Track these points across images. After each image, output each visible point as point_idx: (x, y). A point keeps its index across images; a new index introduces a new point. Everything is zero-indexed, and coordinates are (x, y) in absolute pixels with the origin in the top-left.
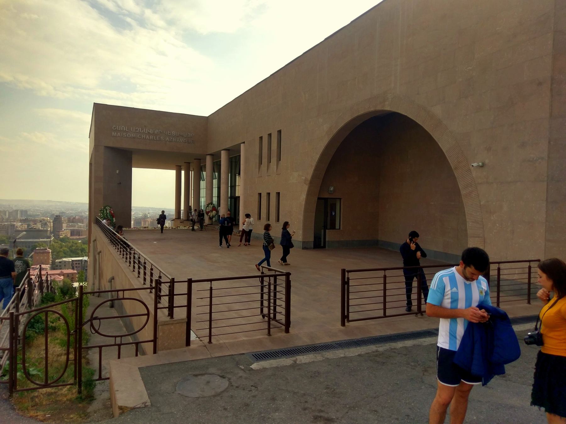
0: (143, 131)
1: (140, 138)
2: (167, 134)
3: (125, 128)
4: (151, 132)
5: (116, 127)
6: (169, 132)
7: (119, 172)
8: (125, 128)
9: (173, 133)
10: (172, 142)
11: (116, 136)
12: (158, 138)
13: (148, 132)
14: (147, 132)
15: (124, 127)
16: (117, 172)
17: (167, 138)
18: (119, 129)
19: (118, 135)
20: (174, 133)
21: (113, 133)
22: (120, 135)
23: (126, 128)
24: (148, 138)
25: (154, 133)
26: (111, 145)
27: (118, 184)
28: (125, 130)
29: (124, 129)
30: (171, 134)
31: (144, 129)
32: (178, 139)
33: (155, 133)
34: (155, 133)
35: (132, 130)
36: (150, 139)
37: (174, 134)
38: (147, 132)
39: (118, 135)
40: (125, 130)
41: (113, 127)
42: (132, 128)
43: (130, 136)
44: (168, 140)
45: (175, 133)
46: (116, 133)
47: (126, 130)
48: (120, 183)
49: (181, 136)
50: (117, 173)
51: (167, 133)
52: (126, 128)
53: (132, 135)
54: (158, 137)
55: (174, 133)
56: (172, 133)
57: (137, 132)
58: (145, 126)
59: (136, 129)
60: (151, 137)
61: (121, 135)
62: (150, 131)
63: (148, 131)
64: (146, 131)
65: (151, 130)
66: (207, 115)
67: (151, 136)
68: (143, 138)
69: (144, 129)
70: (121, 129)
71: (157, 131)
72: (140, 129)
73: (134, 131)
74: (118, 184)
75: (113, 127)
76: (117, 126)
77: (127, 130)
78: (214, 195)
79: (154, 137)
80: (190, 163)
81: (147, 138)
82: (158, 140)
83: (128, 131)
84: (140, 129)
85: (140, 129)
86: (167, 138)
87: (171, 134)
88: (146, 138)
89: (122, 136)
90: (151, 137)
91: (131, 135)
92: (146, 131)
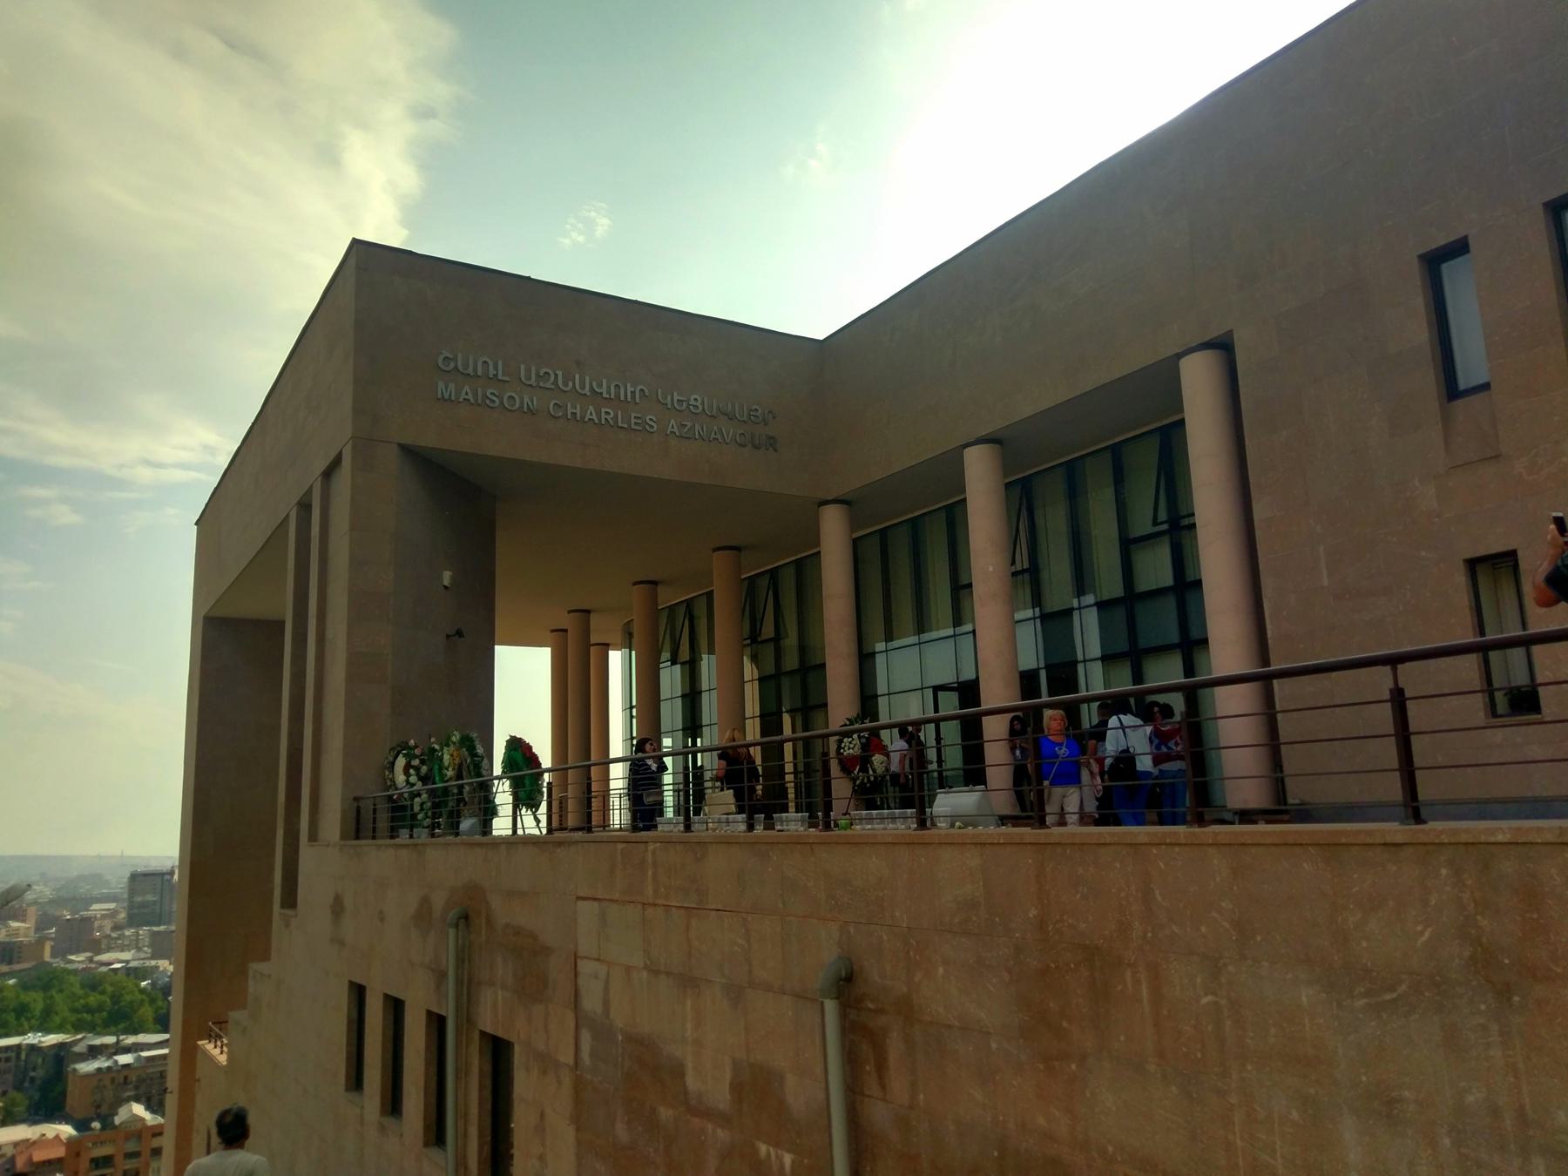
0: (570, 384)
1: (560, 414)
2: (669, 406)
3: (496, 368)
4: (604, 390)
5: (455, 359)
6: (676, 398)
7: (453, 578)
8: (496, 368)
9: (692, 402)
10: (689, 438)
11: (453, 398)
12: (633, 421)
13: (592, 388)
14: (587, 391)
15: (488, 360)
16: (447, 578)
17: (673, 421)
18: (466, 366)
19: (463, 396)
20: (696, 399)
21: (441, 385)
22: (470, 397)
23: (500, 363)
24: (594, 417)
25: (617, 395)
26: (428, 439)
27: (448, 636)
28: (496, 375)
29: (492, 372)
30: (685, 404)
31: (577, 376)
32: (715, 428)
33: (622, 398)
34: (622, 398)
35: (523, 379)
36: (603, 422)
37: (696, 407)
38: (587, 391)
39: (463, 396)
40: (496, 375)
41: (441, 358)
42: (522, 367)
43: (517, 405)
44: (676, 430)
45: (703, 403)
46: (452, 386)
47: (500, 377)
48: (459, 633)
49: (726, 414)
50: (446, 582)
51: (669, 397)
52: (500, 363)
53: (526, 400)
54: (633, 415)
55: (698, 404)
56: (689, 400)
57: (548, 385)
58: (578, 363)
59: (541, 374)
60: (607, 413)
61: (476, 400)
62: (600, 385)
63: (594, 384)
64: (583, 386)
65: (604, 381)
66: (821, 335)
67: (603, 410)
68: (574, 414)
69: (577, 376)
70: (475, 370)
71: (630, 389)
72: (560, 373)
73: (533, 381)
74: (448, 636)
75: (441, 358)
76: (460, 356)
77: (503, 375)
78: (748, 713)
79: (616, 416)
80: (588, 612)
81: (588, 416)
82: (633, 427)
83: (507, 379)
84: (560, 373)
85: (556, 375)
86: (673, 421)
87: (685, 404)
88: (583, 418)
89: (480, 401)
90: (608, 413)
91: (522, 403)
92: (583, 386)
